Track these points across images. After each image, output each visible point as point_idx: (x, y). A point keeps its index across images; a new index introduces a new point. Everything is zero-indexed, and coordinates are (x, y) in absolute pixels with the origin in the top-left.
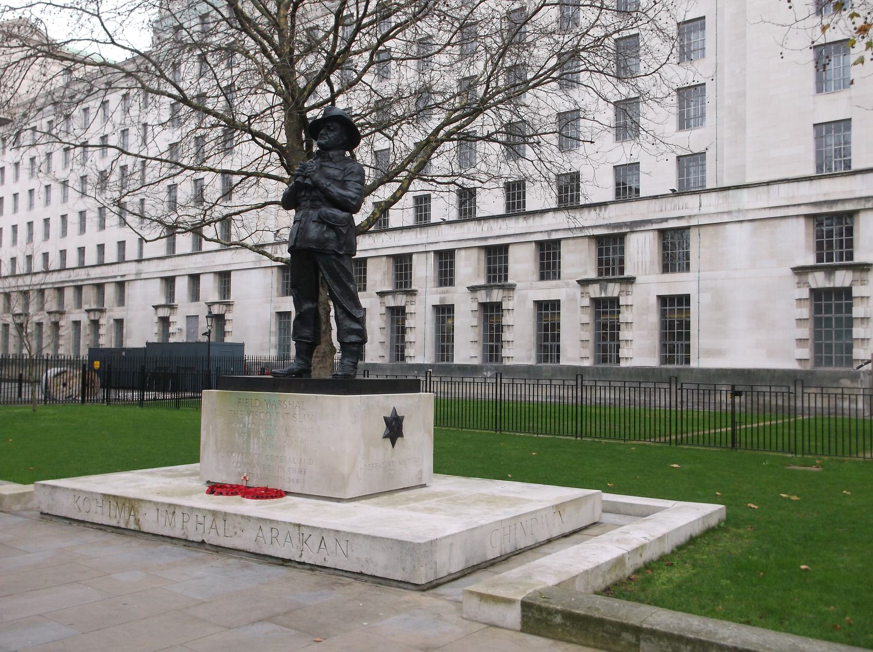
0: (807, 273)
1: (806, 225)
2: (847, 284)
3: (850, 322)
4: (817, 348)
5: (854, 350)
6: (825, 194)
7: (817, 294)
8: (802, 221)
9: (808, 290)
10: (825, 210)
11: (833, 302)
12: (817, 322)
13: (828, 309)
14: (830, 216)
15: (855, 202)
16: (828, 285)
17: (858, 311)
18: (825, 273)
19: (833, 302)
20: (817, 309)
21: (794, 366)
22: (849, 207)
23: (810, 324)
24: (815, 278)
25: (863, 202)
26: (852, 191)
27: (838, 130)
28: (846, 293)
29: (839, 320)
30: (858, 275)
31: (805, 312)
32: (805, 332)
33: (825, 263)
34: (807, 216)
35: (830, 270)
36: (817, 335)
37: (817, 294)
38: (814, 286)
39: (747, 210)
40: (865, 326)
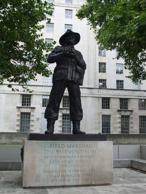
3: (29, 121)
4: (21, 127)
5: (30, 128)
7: (22, 113)
8: (19, 95)
11: (26, 116)
12: (21, 121)
13: (24, 117)
17: (32, 118)
19: (26, 116)
20: (22, 117)
21: (16, 132)
23: (20, 121)
28: (29, 114)
29: (27, 120)
30: (32, 110)
31: (19, 118)
32: (19, 123)
34: (21, 94)
36: (21, 124)
37: (22, 113)
39: (6, 91)
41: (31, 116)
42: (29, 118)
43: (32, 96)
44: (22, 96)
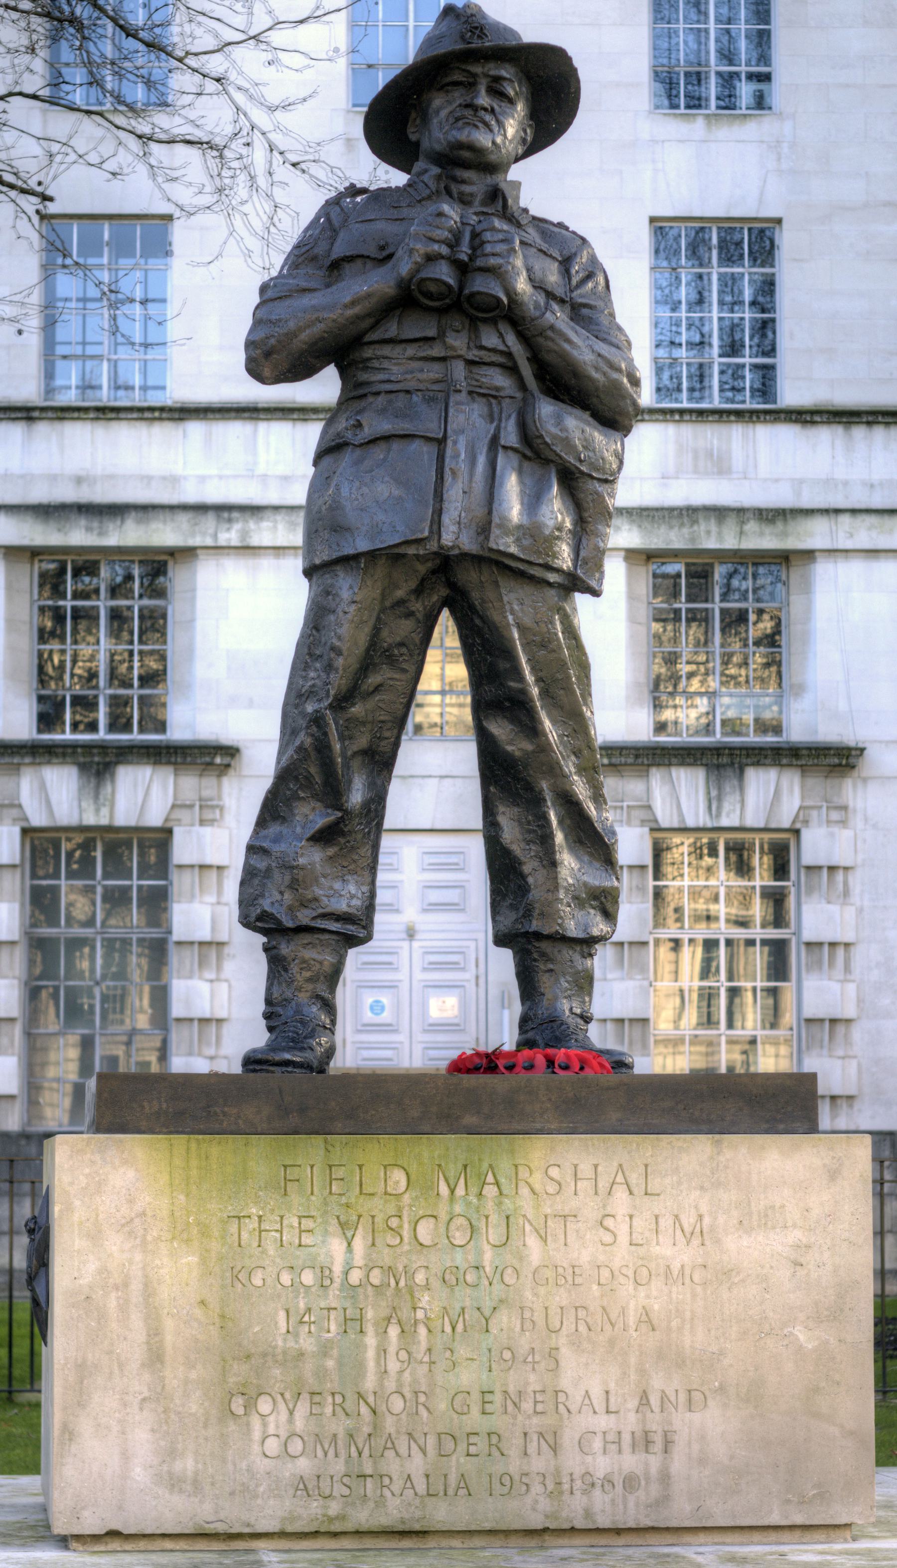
0: (16, 769)
1: (10, 588)
2: (155, 818)
6: (79, 480)
9: (17, 830)
10: (78, 536)
14: (86, 563)
15: (183, 519)
16: (90, 819)
18: (83, 768)
22: (164, 534)
24: (43, 787)
25: (209, 521)
26: (173, 480)
27: (122, 248)
30: (190, 784)
33: (68, 736)
35: (98, 764)
38: (38, 819)
40: (210, 975)
41: (180, 882)
42: (157, 902)
43: (176, 577)
44: (27, 576)
